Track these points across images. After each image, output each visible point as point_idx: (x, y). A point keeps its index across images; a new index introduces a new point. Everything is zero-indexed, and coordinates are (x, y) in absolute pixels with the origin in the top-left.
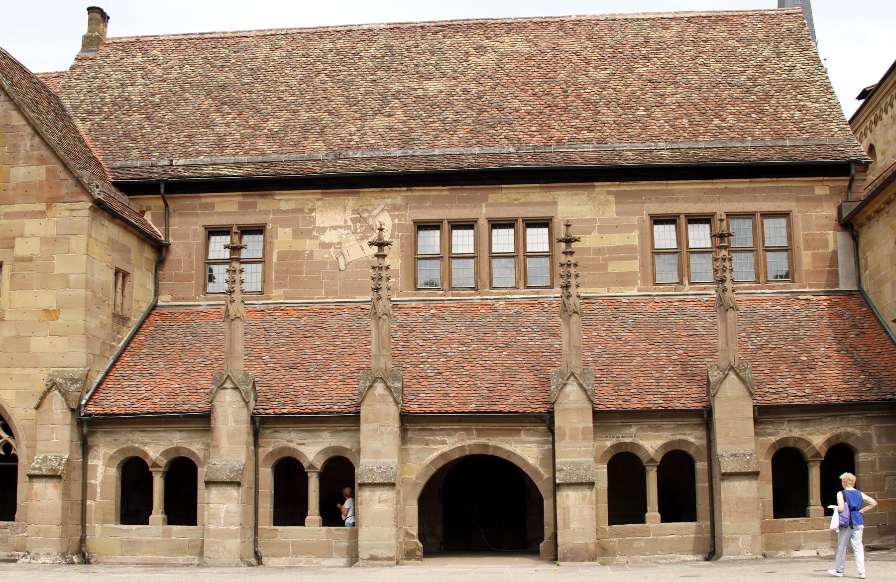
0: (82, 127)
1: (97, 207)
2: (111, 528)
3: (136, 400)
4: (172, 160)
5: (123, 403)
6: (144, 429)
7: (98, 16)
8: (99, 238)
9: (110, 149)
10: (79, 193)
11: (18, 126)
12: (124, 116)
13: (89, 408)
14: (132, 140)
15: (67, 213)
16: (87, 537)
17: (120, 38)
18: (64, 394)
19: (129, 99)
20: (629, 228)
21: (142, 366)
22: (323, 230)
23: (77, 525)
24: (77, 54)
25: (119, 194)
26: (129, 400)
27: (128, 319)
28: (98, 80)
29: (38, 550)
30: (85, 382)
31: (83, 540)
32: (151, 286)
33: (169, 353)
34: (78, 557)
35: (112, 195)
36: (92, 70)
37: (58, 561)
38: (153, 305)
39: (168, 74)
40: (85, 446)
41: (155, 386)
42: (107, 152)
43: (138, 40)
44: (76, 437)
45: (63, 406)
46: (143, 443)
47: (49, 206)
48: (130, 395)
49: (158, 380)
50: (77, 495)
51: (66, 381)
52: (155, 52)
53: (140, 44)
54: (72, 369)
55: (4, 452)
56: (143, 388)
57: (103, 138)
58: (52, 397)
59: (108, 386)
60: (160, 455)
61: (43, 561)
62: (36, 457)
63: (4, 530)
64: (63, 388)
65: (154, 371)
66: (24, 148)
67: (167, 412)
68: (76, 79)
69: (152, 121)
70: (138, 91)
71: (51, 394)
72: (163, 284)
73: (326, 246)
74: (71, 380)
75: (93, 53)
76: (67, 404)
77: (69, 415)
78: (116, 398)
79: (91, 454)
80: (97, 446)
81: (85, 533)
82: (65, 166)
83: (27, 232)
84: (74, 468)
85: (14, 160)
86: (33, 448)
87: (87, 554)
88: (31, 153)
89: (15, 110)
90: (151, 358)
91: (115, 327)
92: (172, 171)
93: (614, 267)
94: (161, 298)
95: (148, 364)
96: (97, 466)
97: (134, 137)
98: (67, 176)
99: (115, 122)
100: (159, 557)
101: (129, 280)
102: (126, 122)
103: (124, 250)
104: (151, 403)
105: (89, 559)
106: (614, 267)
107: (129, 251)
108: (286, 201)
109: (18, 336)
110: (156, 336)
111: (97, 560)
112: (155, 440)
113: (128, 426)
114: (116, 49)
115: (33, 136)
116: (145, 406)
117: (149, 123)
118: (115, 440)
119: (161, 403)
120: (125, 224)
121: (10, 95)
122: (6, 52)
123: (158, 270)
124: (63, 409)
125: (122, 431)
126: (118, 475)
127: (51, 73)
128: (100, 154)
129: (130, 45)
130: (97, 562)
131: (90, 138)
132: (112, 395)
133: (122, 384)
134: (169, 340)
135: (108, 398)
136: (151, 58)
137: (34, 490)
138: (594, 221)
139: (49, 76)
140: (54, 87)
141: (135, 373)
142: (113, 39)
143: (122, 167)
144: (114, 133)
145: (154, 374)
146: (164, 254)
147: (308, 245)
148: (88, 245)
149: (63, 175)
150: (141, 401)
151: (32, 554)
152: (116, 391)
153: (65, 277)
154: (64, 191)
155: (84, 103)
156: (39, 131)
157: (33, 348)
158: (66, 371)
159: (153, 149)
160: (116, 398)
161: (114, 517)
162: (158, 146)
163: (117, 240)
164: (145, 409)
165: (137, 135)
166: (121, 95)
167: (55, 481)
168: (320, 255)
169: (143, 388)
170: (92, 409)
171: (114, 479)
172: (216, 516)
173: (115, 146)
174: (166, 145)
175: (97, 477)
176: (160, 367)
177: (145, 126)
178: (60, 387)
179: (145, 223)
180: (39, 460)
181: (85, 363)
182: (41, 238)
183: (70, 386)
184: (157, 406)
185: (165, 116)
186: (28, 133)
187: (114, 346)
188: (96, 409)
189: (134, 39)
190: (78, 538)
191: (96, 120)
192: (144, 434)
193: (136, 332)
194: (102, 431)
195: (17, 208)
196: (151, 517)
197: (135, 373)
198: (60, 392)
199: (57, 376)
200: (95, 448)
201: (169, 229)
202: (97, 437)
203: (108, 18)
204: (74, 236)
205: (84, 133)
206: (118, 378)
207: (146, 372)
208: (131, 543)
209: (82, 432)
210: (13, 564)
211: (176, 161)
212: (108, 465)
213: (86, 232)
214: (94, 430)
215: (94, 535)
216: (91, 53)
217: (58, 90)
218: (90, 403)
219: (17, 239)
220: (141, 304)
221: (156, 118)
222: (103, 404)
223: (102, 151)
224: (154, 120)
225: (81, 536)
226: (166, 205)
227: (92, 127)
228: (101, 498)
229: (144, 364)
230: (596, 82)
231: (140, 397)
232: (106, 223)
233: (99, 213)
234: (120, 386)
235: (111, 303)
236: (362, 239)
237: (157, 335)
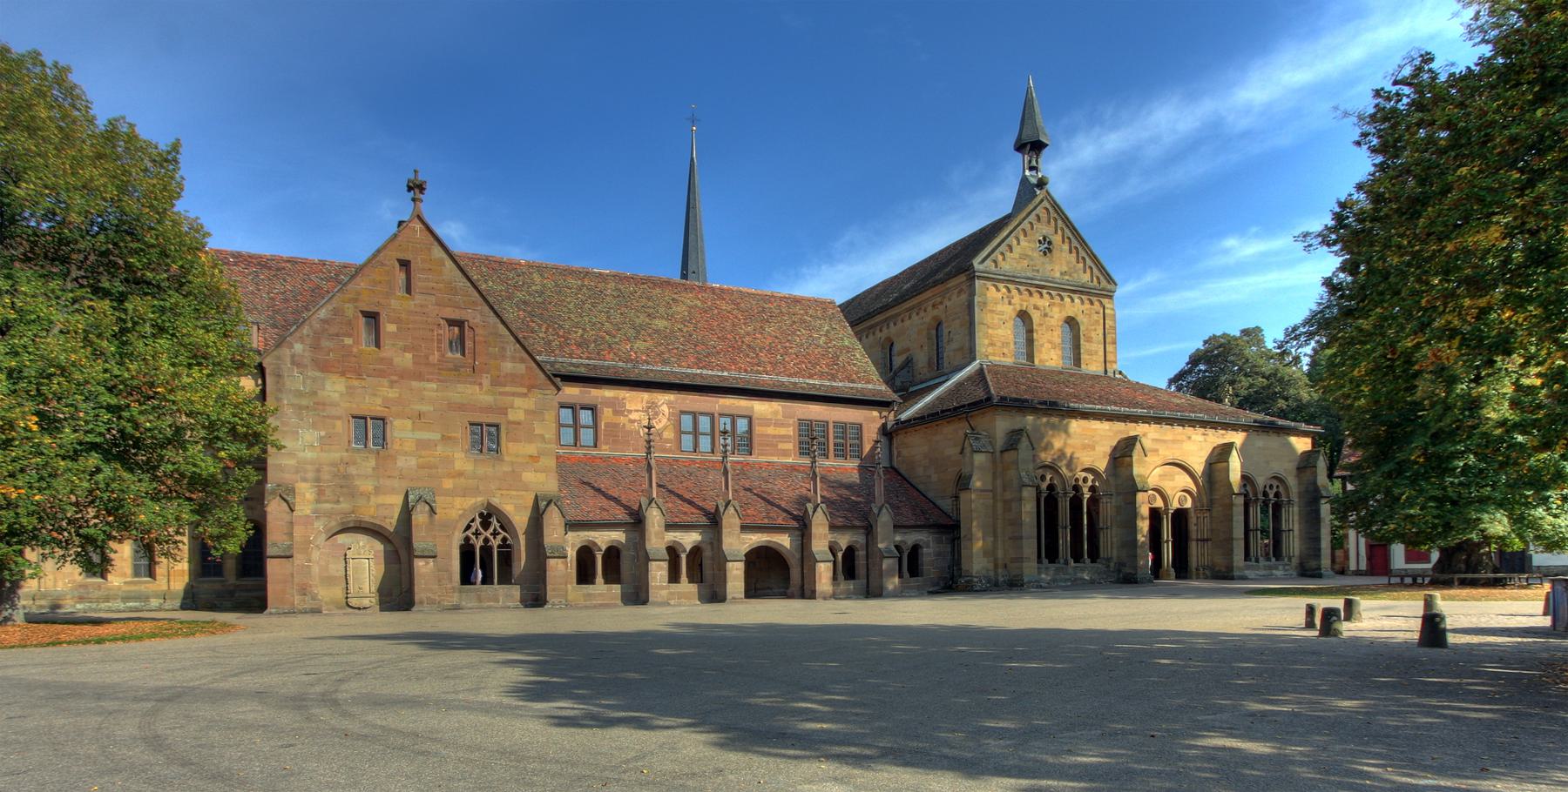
20: (789, 425)
47: (529, 390)
73: (633, 421)
85: (503, 357)
93: (781, 446)
106: (781, 446)
108: (608, 393)
138: (771, 419)
147: (622, 420)
168: (629, 427)
172: (655, 578)
182: (525, 411)
195: (507, 389)
230: (748, 334)
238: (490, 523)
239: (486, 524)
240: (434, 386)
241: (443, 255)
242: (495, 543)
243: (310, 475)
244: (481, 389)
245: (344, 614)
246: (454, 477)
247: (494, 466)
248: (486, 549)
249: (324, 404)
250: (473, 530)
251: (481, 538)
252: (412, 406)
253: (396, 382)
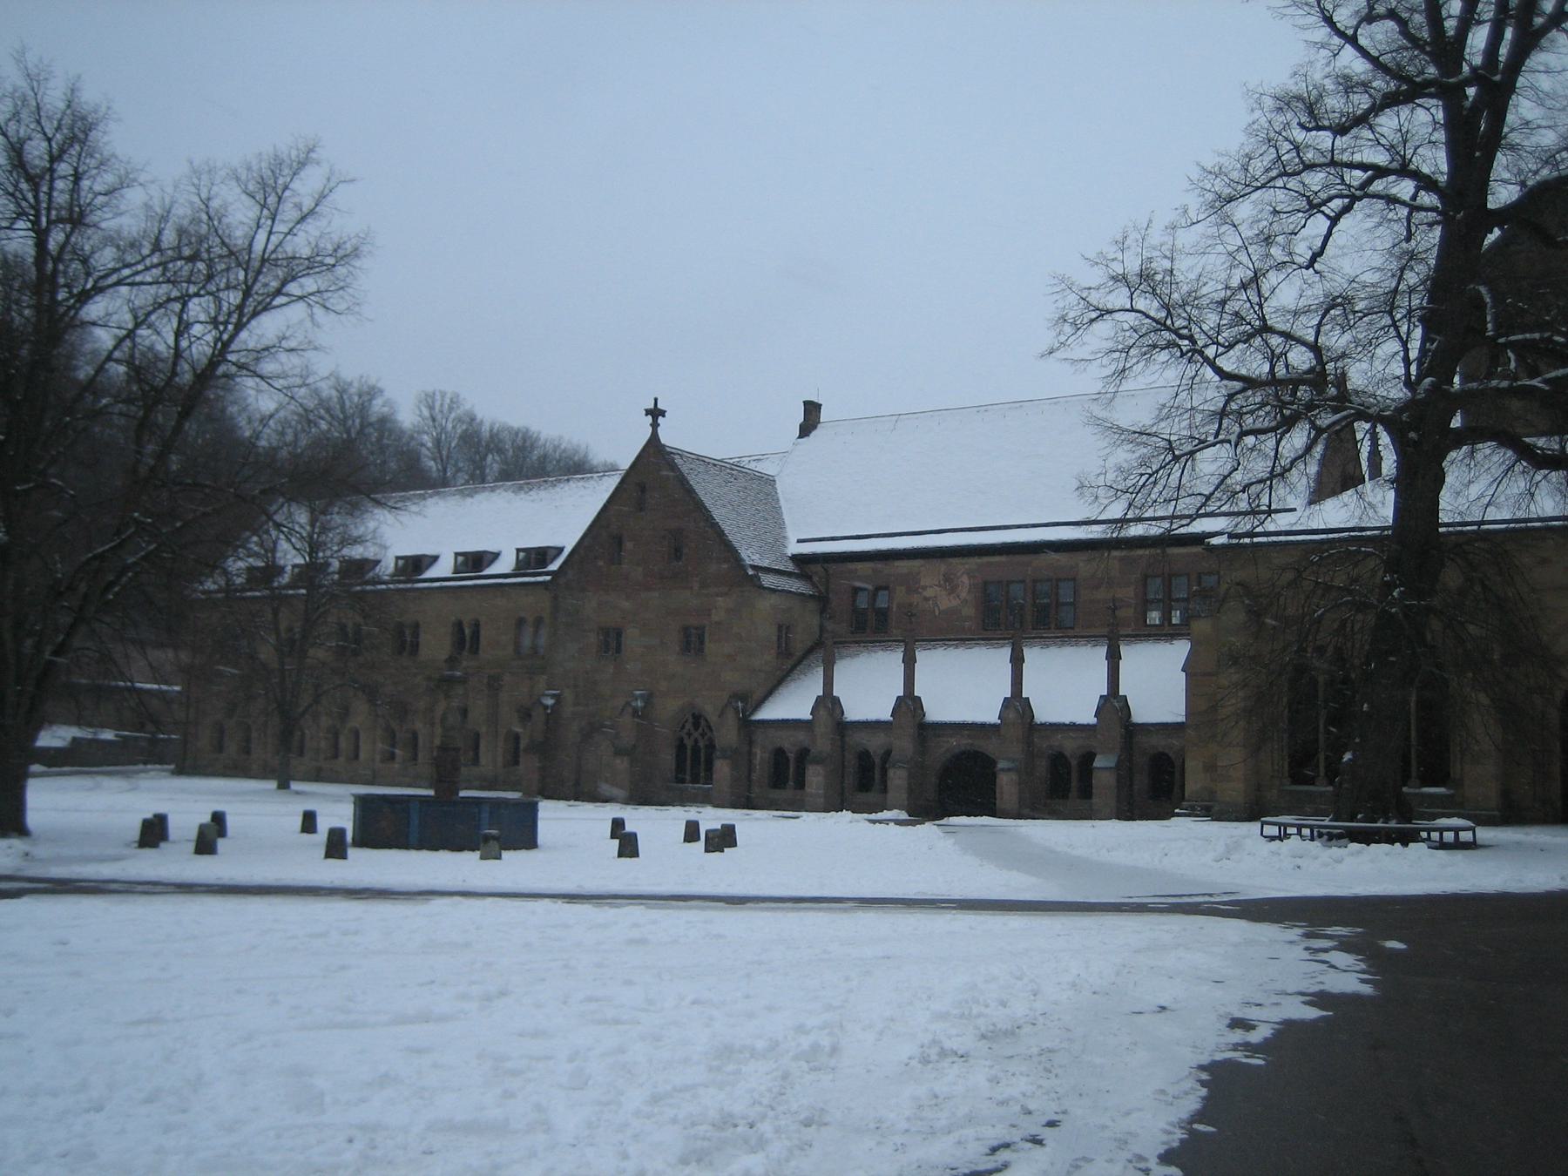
22: (924, 588)
73: (927, 599)
147: (915, 599)
235: (776, 645)
236: (949, 594)
239: (696, 725)
240: (656, 594)
242: (701, 744)
245: (570, 806)
248: (696, 750)
250: (685, 731)
251: (692, 738)
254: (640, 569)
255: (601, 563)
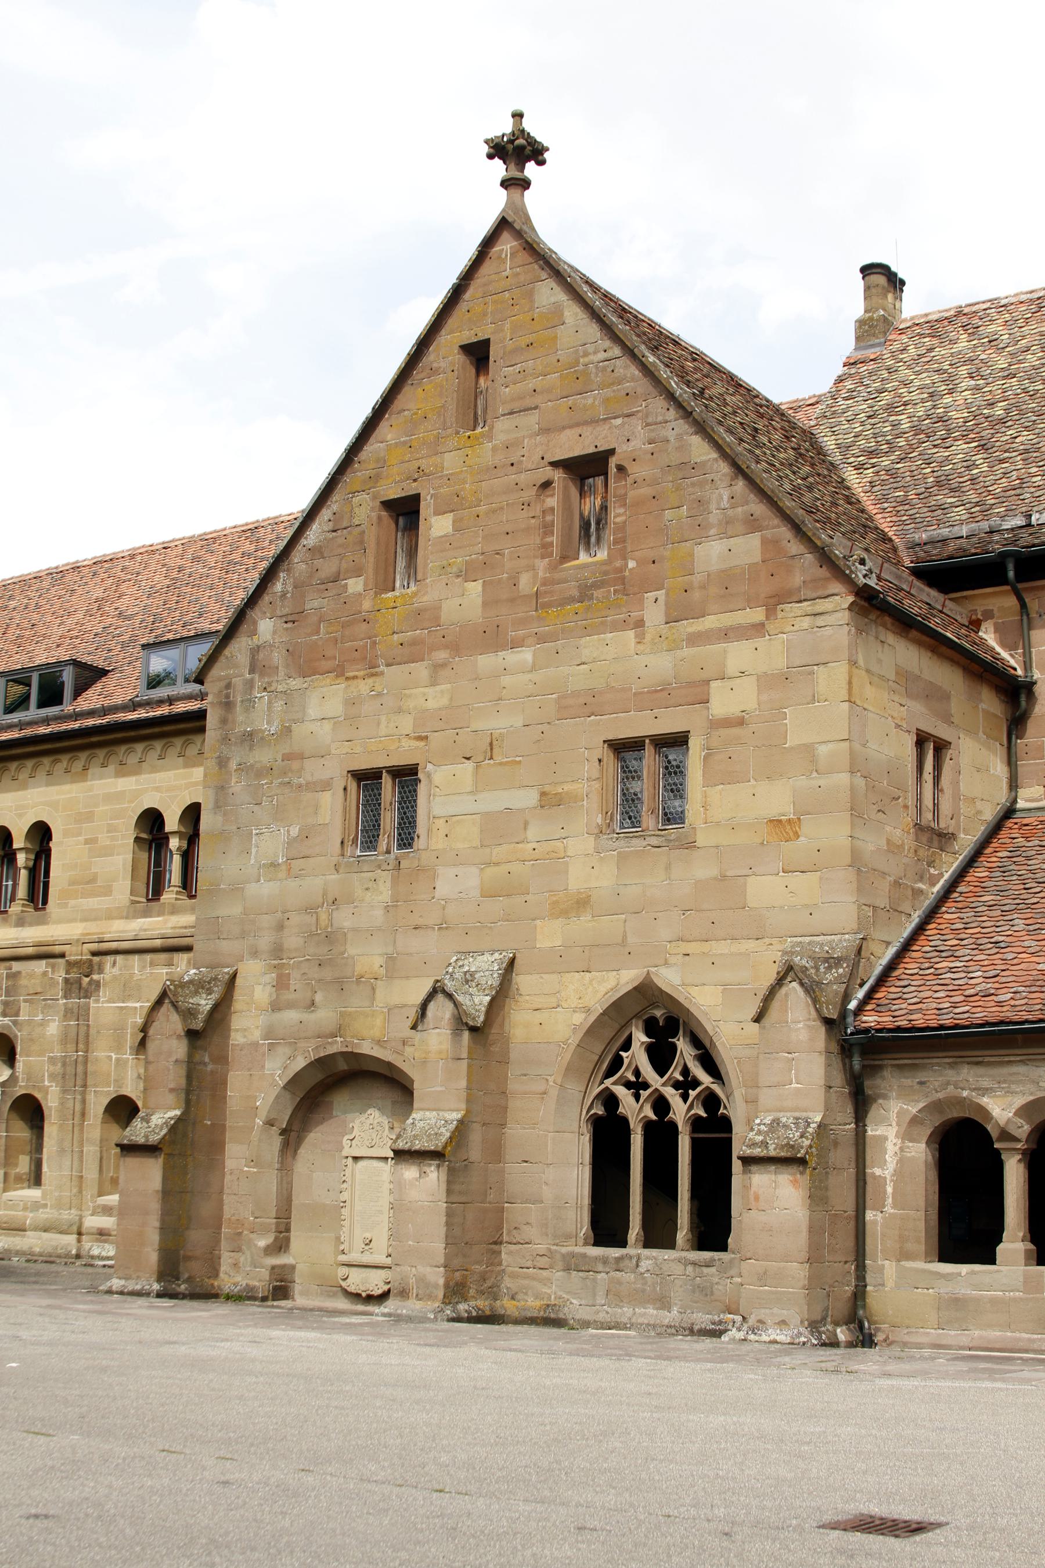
0: (858, 481)
1: (866, 605)
2: (917, 1270)
3: (962, 998)
4: (1031, 516)
5: (935, 1005)
6: (980, 1059)
7: (881, 280)
8: (875, 668)
9: (911, 512)
10: (826, 579)
11: (704, 464)
12: (936, 450)
13: (865, 1018)
14: (952, 490)
15: (806, 623)
16: (869, 1288)
17: (926, 315)
18: (811, 989)
19: (945, 418)
21: (978, 930)
23: (846, 1262)
24: (848, 354)
25: (927, 589)
26: (947, 999)
27: (953, 836)
28: (886, 393)
29: (763, 1313)
30: (855, 965)
31: (859, 1295)
32: (999, 769)
33: (1035, 900)
34: (849, 1329)
35: (905, 587)
36: (874, 378)
37: (803, 1339)
38: (1005, 808)
39: (1020, 362)
40: (860, 1097)
41: (1003, 967)
42: (905, 518)
43: (959, 313)
44: (839, 1079)
45: (810, 1014)
46: (979, 1089)
47: (771, 611)
48: (950, 987)
49: (1010, 956)
50: (843, 1198)
51: (816, 963)
52: (992, 328)
53: (965, 319)
54: (829, 938)
55: (706, 1112)
56: (979, 974)
57: (897, 494)
58: (786, 995)
59: (907, 972)
60: (1015, 1114)
61: (772, 1338)
62: (758, 1121)
63: (706, 1270)
64: (809, 977)
65: (1002, 938)
66: (718, 503)
67: (1027, 1022)
68: (846, 399)
69: (990, 451)
70: (962, 402)
71: (784, 990)
72: (1025, 765)
74: (826, 960)
75: (877, 349)
76: (817, 1010)
77: (822, 1031)
78: (922, 995)
79: (874, 1113)
80: (885, 1097)
81: (864, 1278)
82: (797, 528)
83: (732, 669)
84: (836, 1144)
85: (700, 530)
86: (752, 1101)
87: (866, 1324)
88: (730, 512)
89: (696, 433)
90: (999, 913)
91: (922, 853)
92: (1031, 534)
94: (1023, 793)
95: (992, 923)
96: (886, 1138)
97: (957, 485)
98: (802, 547)
99: (920, 462)
100: (1017, 1335)
101: (948, 757)
102: (940, 459)
103: (934, 696)
104: (993, 1004)
105: (871, 1335)
107: (946, 697)
109: (724, 877)
110: (1011, 868)
111: (887, 1337)
112: (1005, 1082)
113: (944, 1054)
114: (919, 334)
115: (732, 479)
116: (979, 1009)
117: (985, 456)
118: (921, 1083)
119: (1013, 1002)
120: (932, 642)
121: (685, 404)
122: (702, 353)
123: (1014, 737)
124: (809, 1019)
125: (933, 1065)
126: (930, 1157)
127: (804, 399)
128: (892, 524)
129: (946, 323)
130: (888, 1342)
131: (872, 498)
132: (913, 989)
133: (936, 966)
134: (1038, 876)
135: (905, 996)
136: (986, 340)
137: (753, 1189)
139: (801, 404)
140: (803, 419)
141: (963, 943)
142: (912, 318)
143: (931, 542)
144: (917, 482)
145: (1002, 945)
146: (1023, 704)
148: (850, 683)
149: (795, 547)
150: (972, 999)
151: (752, 1320)
152: (922, 982)
153: (808, 750)
154: (797, 579)
155: (860, 438)
156: (744, 467)
157: (752, 902)
158: (818, 943)
159: (993, 501)
160: (922, 995)
161: (922, 1248)
162: (1002, 494)
163: (917, 672)
164: (979, 1015)
165: (961, 480)
166: (930, 413)
167: (794, 1169)
169: (979, 974)
170: (870, 1019)
171: (922, 1167)
173: (920, 505)
174: (1018, 491)
175: (886, 1161)
176: (1015, 928)
177: (977, 463)
178: (800, 975)
179: (983, 642)
180: (762, 1127)
181: (855, 926)
183: (825, 974)
184: (1005, 1009)
185: (1016, 437)
186: (723, 475)
187: (921, 891)
188: (880, 1019)
189: (952, 313)
190: (849, 1289)
191: (883, 464)
192: (981, 1070)
193: (971, 862)
194: (893, 1066)
195: (710, 622)
196: (1000, 1248)
197: (963, 943)
198: (802, 984)
199: (798, 954)
200: (880, 1101)
201: (1030, 653)
202: (883, 1078)
203: (902, 283)
204: (822, 667)
205: (861, 489)
206: (928, 955)
207: (988, 940)
208: (957, 1303)
209: (851, 1067)
210: (708, 1343)
211: (1037, 515)
212: (907, 1136)
213: (846, 655)
214: (877, 1063)
215: (883, 1285)
216: (873, 350)
217: (812, 423)
218: (869, 1007)
219: (714, 685)
220: (979, 805)
221: (998, 444)
222: (894, 1007)
223: (894, 519)
224: (995, 449)
225: (856, 1286)
226: (1023, 605)
227: (876, 478)
228: (895, 1206)
229: (984, 925)
231: (972, 992)
232: (891, 638)
233: (873, 616)
234: (932, 970)
235: (911, 802)
237: (1013, 867)
238: (674, 1048)
240: (526, 655)
241: (560, 296)
242: (680, 1111)
243: (265, 942)
244: (640, 640)
246: (565, 913)
247: (668, 868)
249: (301, 757)
252: (474, 726)
253: (443, 666)
254: (475, 588)
255: (355, 585)
